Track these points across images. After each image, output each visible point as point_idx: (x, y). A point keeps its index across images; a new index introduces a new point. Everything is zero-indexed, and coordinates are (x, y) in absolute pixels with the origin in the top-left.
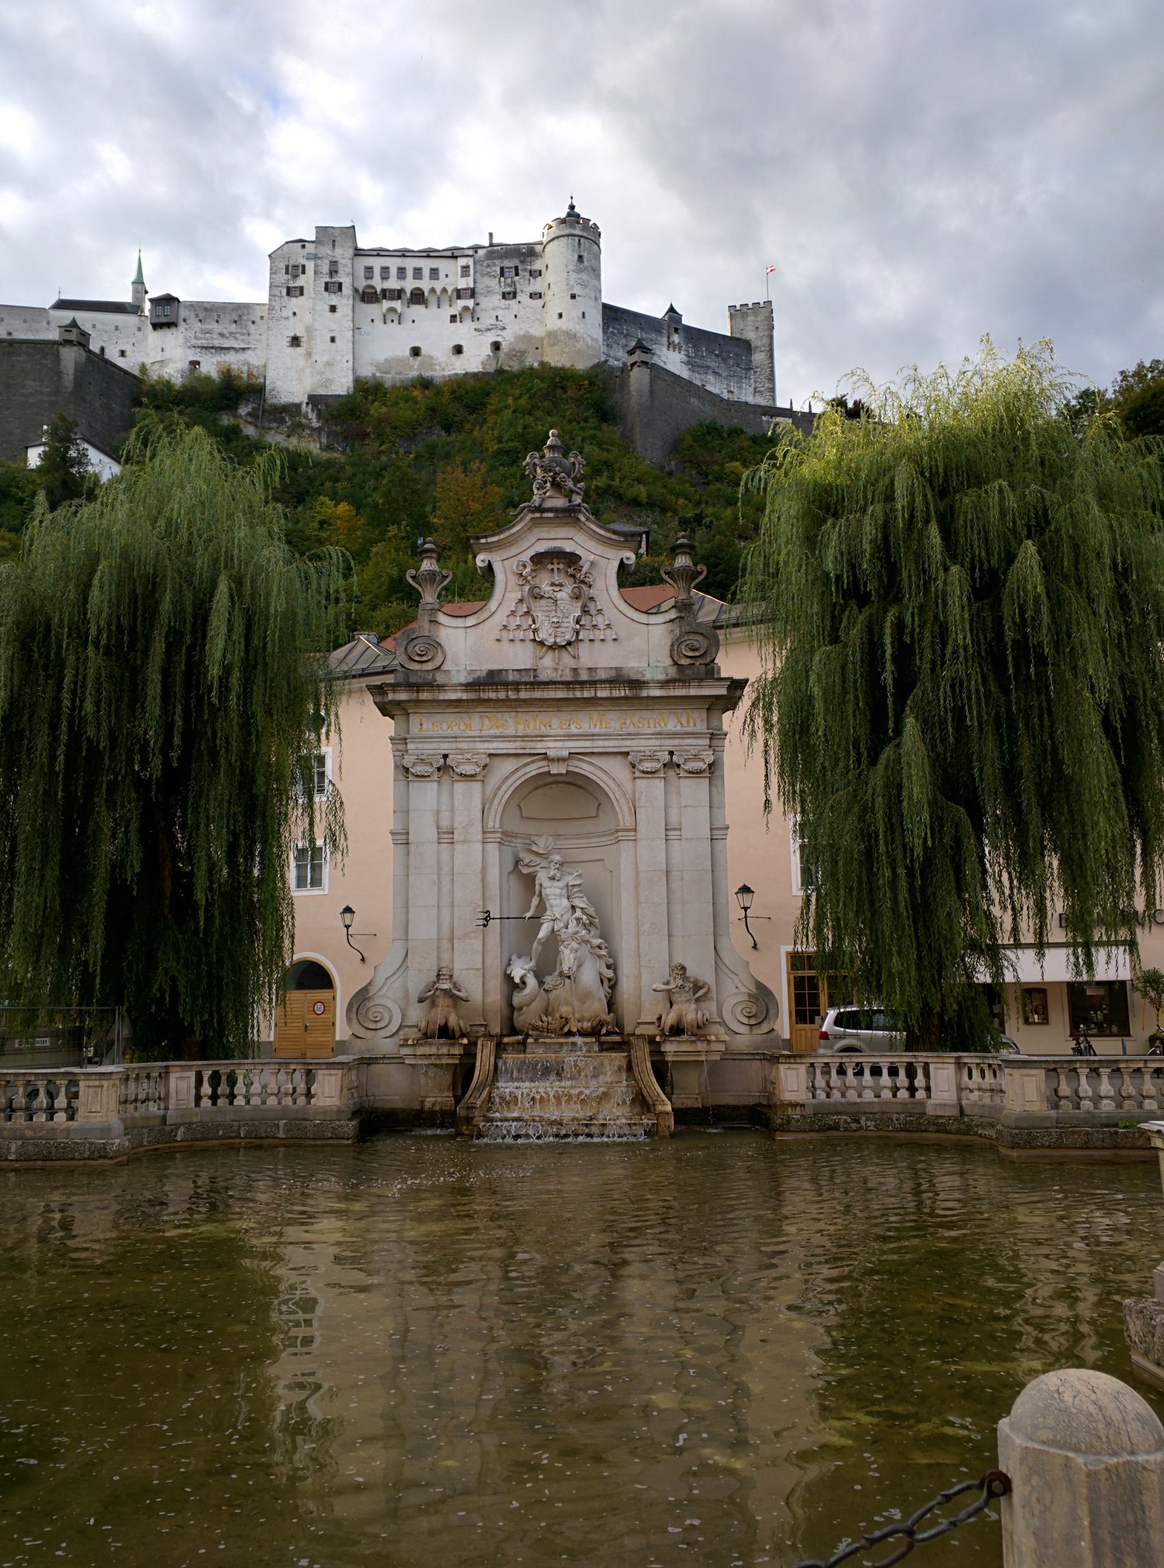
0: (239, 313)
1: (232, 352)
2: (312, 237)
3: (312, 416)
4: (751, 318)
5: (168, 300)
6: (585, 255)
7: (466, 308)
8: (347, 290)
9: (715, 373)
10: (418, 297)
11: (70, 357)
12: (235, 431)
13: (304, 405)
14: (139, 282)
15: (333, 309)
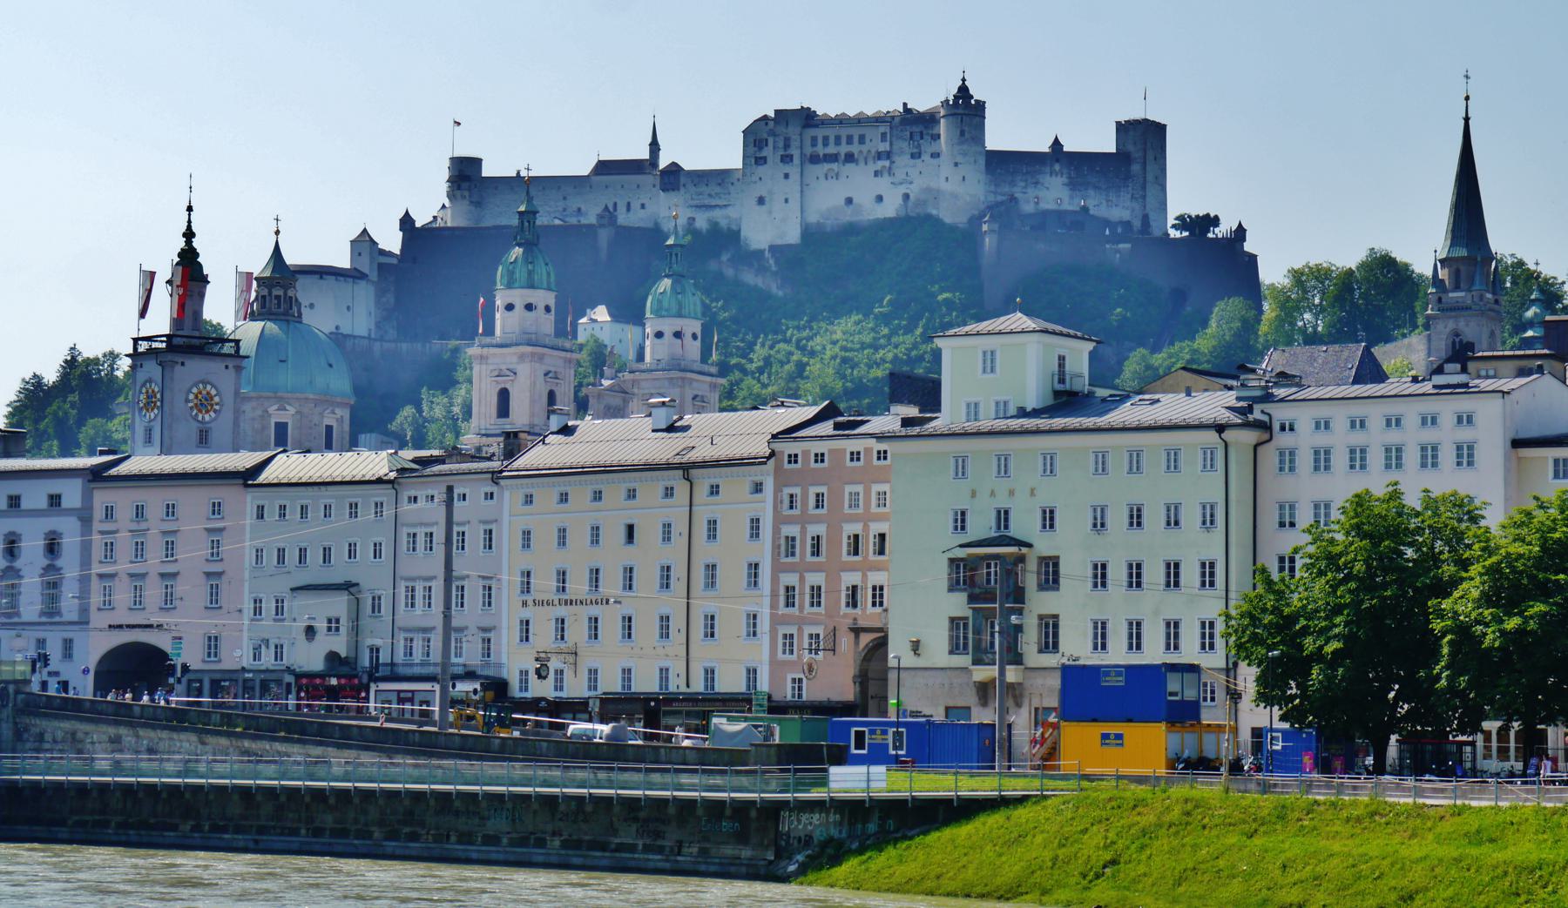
0: (720, 177)
1: (718, 209)
2: (772, 115)
3: (772, 262)
4: (1131, 133)
5: (674, 169)
6: (966, 129)
7: (884, 167)
8: (796, 160)
9: (1096, 188)
10: (850, 158)
11: (604, 236)
12: (720, 276)
13: (767, 252)
14: (654, 146)
15: (786, 176)
